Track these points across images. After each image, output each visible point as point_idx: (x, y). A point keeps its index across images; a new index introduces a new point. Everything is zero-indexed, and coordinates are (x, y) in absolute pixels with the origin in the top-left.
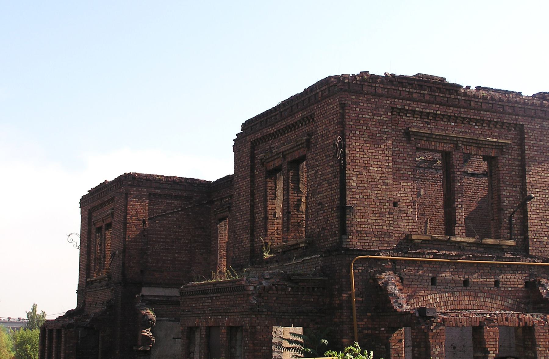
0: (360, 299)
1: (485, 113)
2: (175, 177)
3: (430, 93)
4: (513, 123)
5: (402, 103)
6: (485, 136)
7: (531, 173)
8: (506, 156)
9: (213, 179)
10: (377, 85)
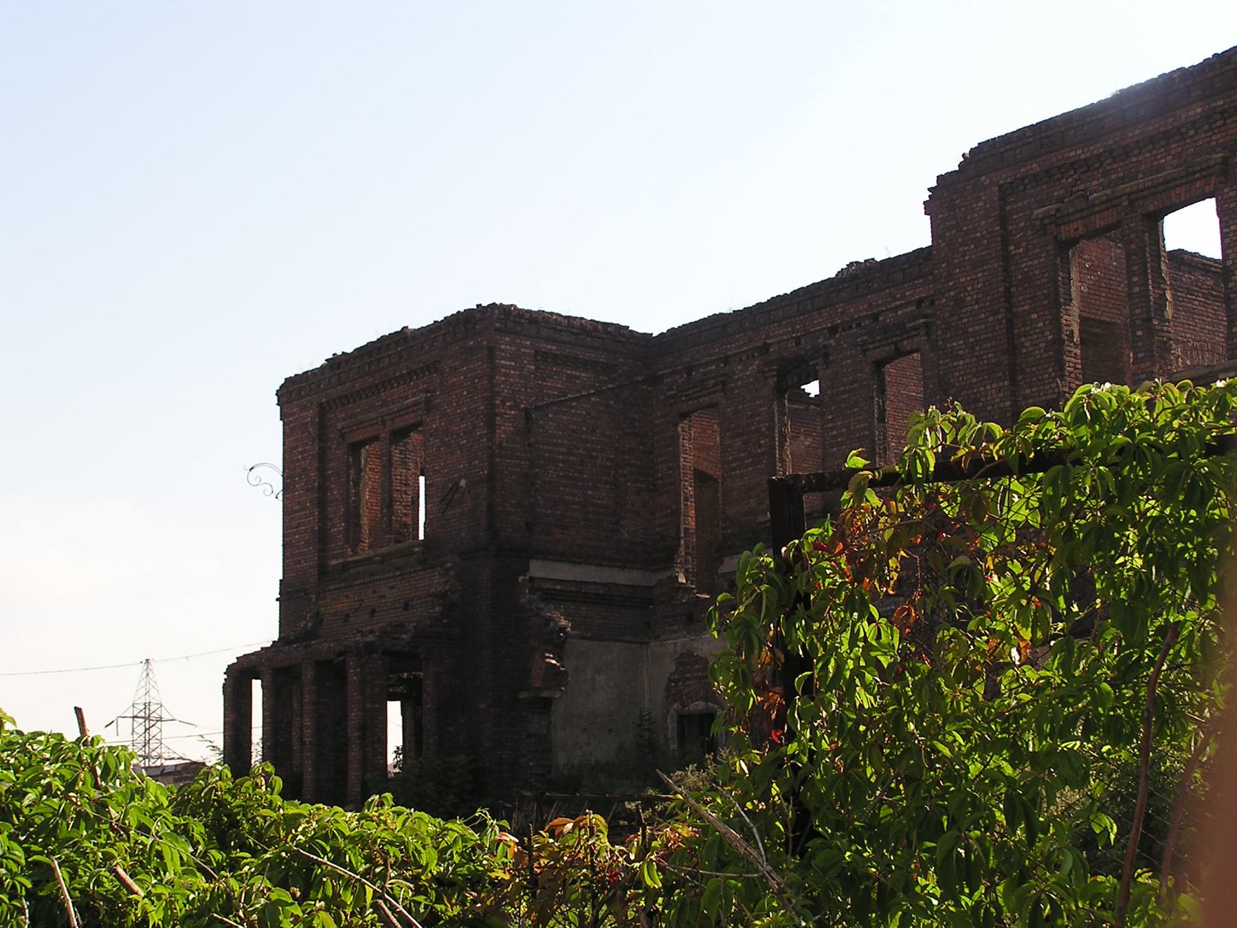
9: (656, 327)
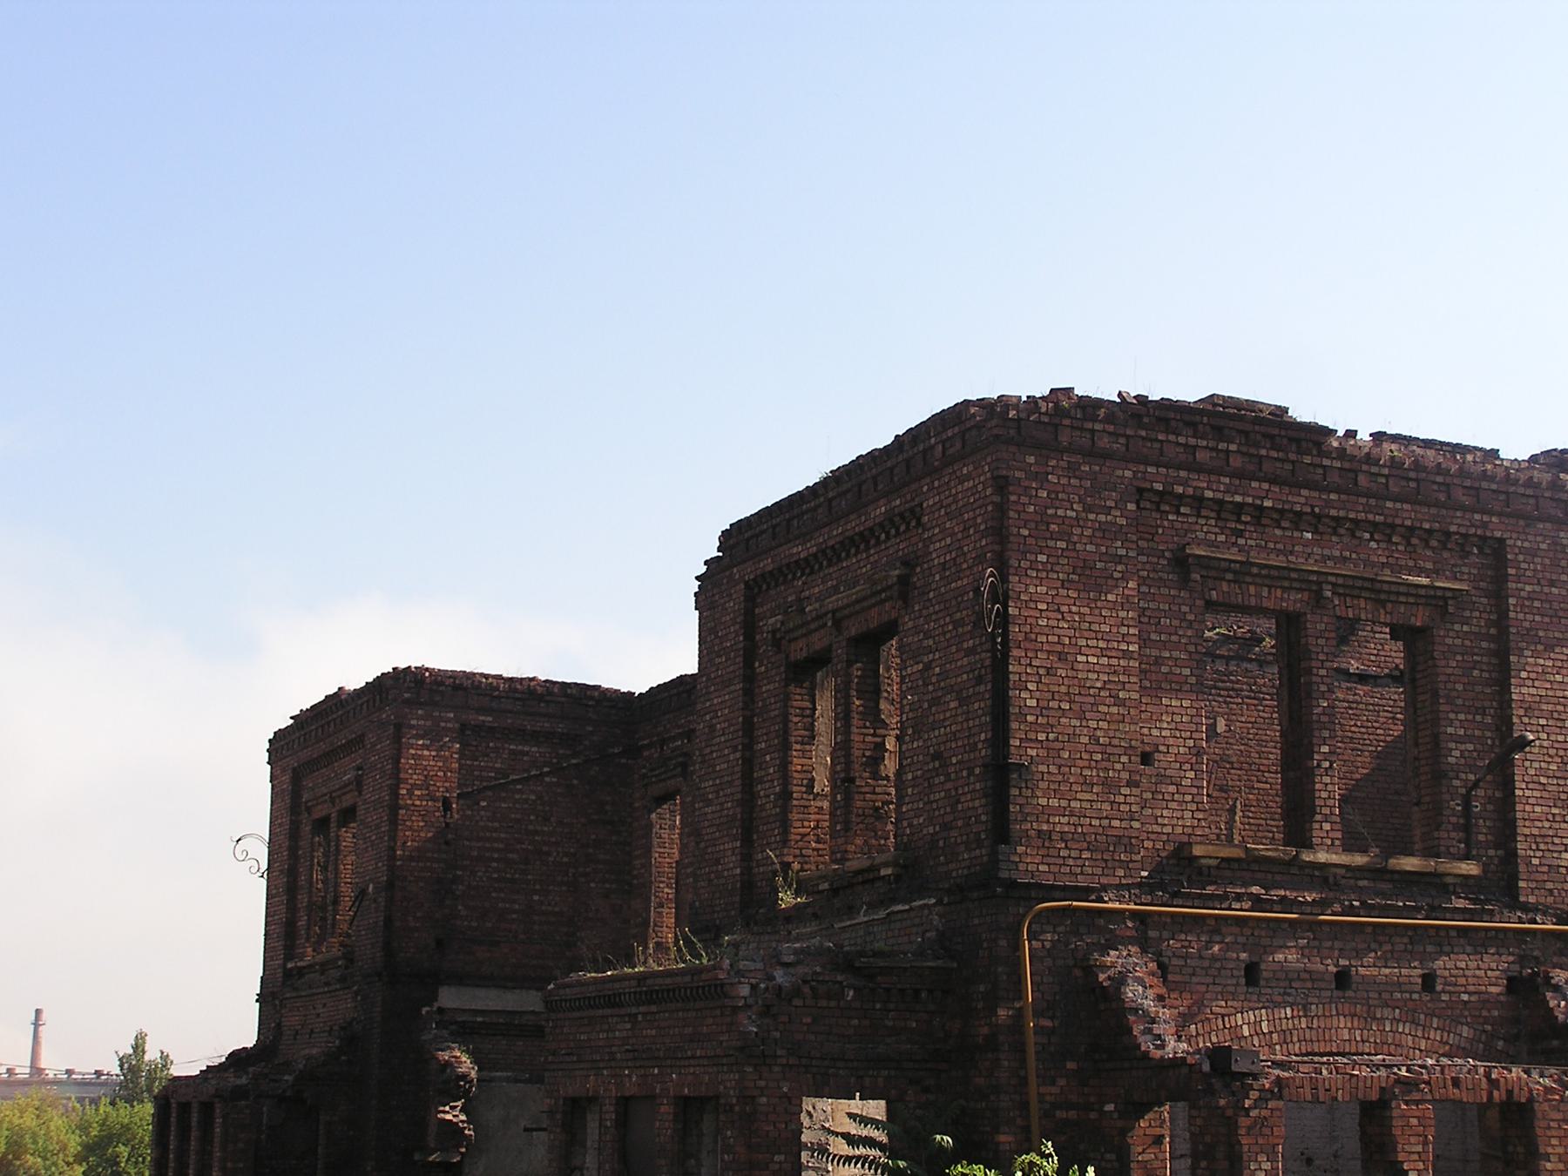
0: (1047, 1023)
1: (1398, 505)
2: (533, 679)
3: (1244, 449)
4: (1475, 535)
5: (1167, 476)
6: (1397, 569)
7: (1524, 674)
8: (1457, 627)
9: (640, 686)
10: (1098, 427)
